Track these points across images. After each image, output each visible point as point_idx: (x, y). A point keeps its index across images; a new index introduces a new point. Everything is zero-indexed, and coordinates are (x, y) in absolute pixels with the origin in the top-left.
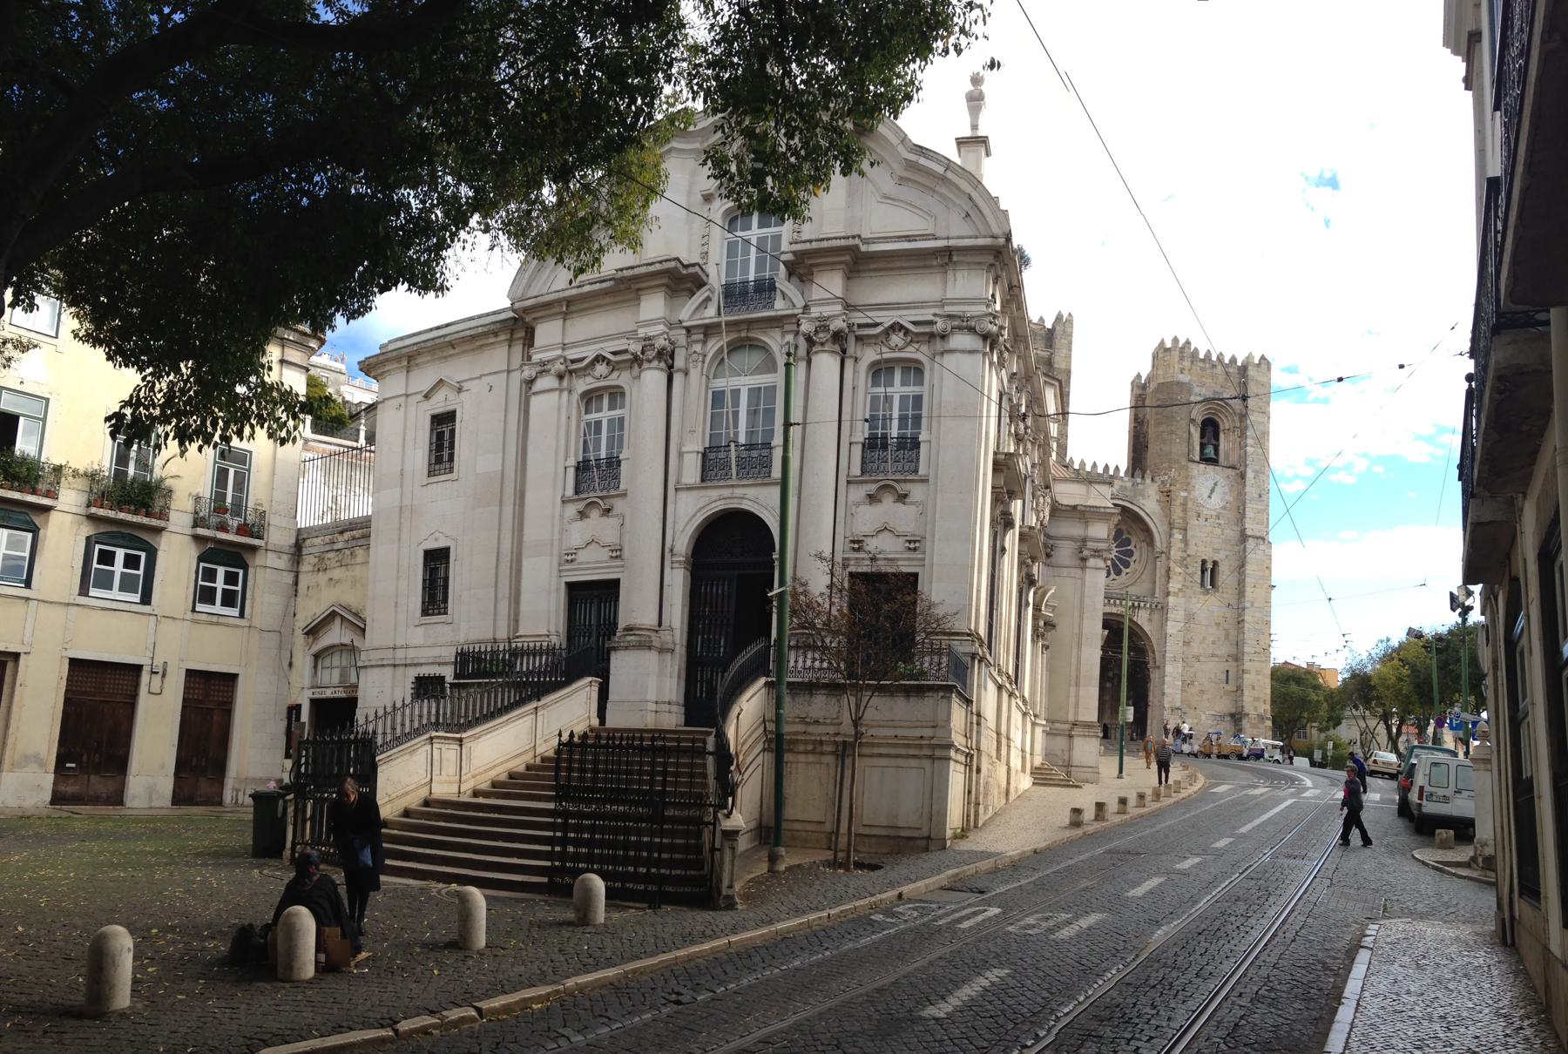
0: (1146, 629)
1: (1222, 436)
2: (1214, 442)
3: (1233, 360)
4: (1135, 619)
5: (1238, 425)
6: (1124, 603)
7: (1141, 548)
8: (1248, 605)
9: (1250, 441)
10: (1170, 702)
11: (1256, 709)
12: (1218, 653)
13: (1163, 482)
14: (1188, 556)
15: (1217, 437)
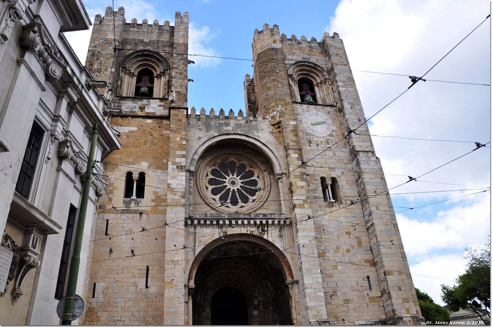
0: (279, 244)
1: (316, 89)
2: (313, 94)
3: (314, 40)
4: (265, 237)
5: (328, 77)
6: (252, 222)
7: (264, 179)
8: (373, 209)
9: (340, 84)
10: (315, 316)
11: (408, 311)
12: (355, 260)
13: (273, 117)
14: (307, 175)
15: (313, 91)
